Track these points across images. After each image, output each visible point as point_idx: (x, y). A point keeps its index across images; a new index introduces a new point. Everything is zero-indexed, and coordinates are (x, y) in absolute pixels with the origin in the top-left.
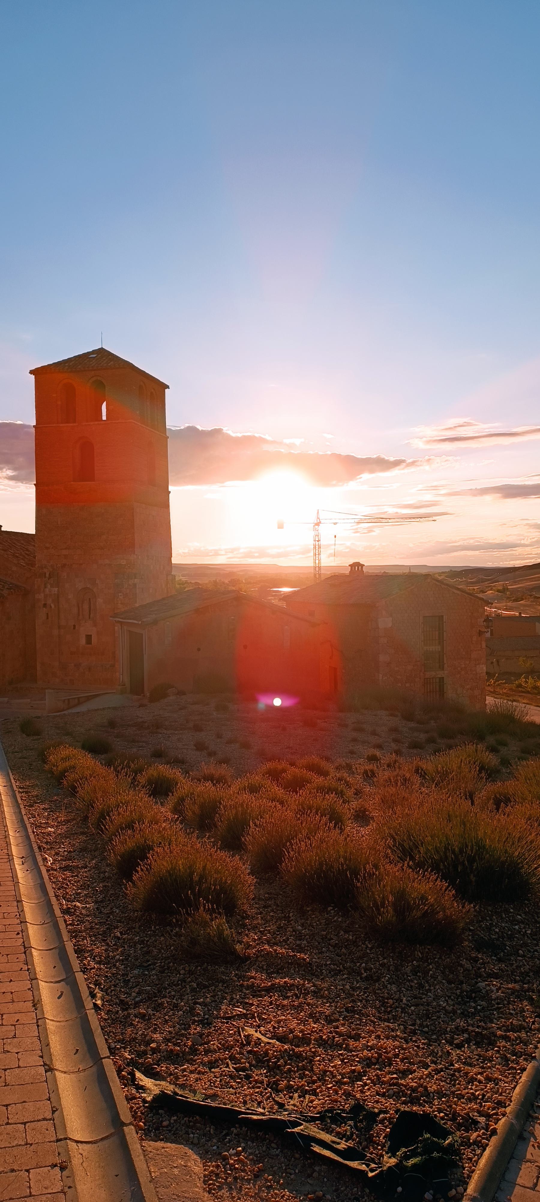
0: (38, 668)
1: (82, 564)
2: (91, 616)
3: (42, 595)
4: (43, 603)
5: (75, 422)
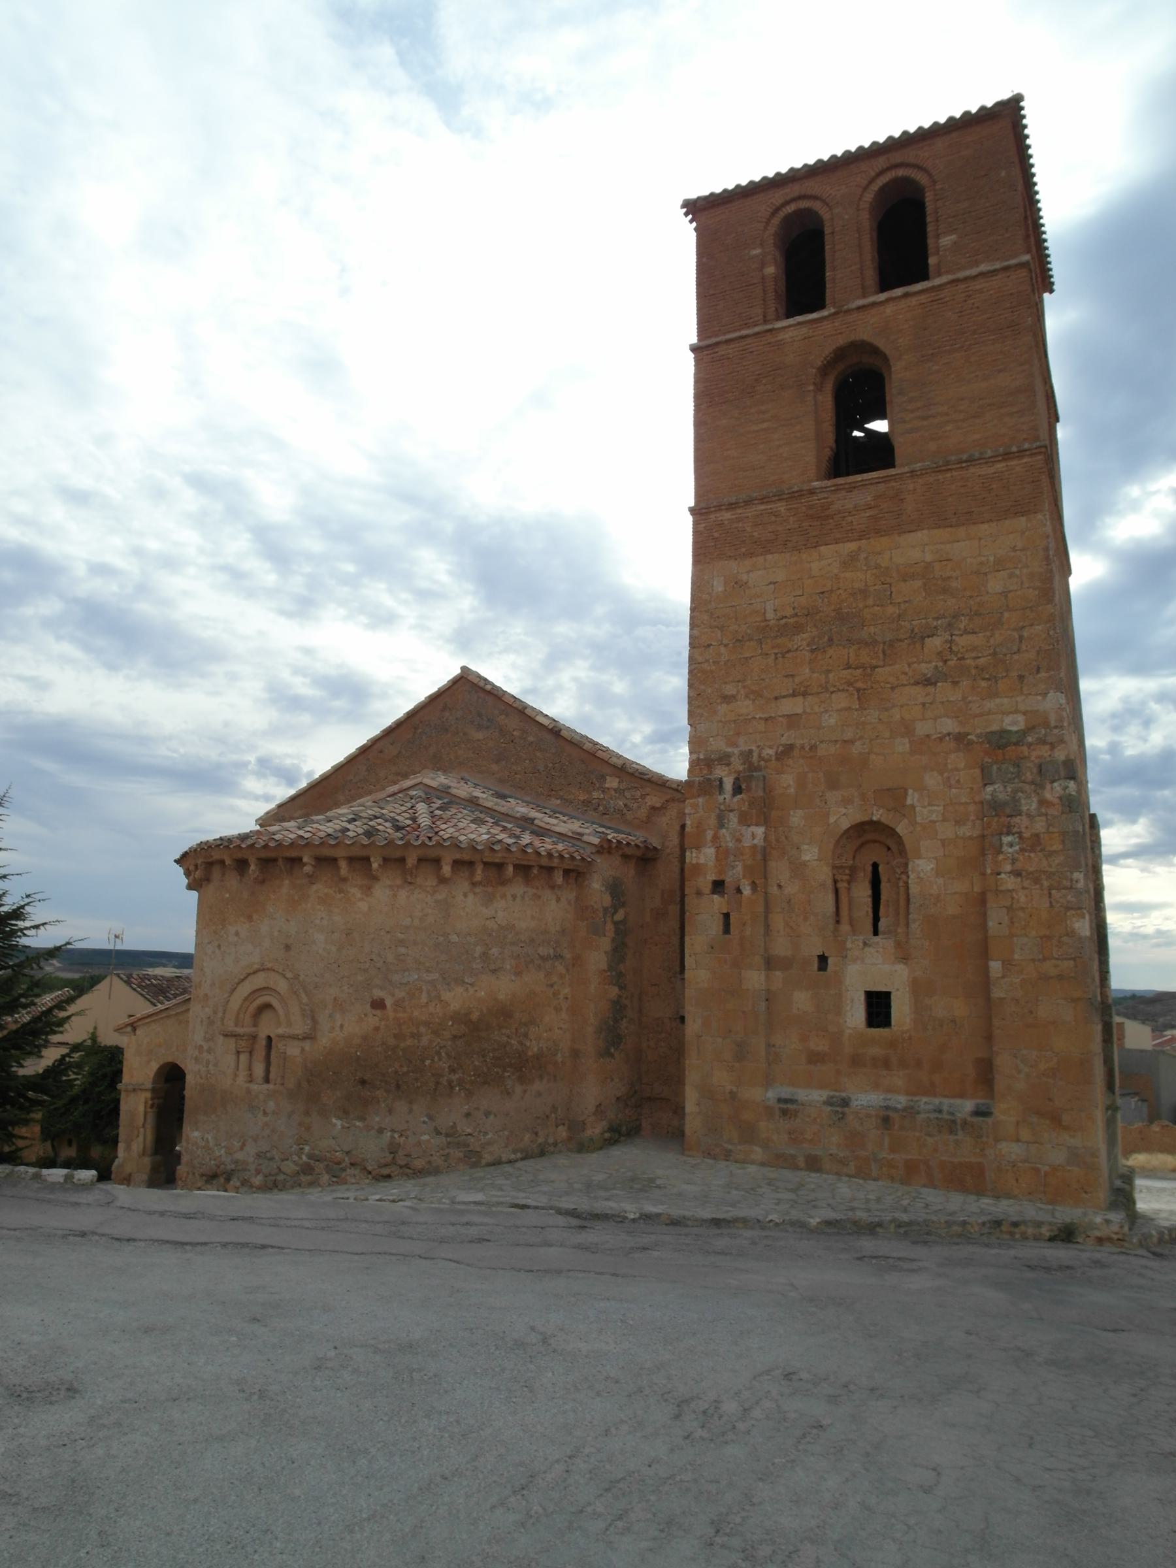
0: (690, 1107)
1: (852, 742)
4: (712, 877)
5: (821, 306)
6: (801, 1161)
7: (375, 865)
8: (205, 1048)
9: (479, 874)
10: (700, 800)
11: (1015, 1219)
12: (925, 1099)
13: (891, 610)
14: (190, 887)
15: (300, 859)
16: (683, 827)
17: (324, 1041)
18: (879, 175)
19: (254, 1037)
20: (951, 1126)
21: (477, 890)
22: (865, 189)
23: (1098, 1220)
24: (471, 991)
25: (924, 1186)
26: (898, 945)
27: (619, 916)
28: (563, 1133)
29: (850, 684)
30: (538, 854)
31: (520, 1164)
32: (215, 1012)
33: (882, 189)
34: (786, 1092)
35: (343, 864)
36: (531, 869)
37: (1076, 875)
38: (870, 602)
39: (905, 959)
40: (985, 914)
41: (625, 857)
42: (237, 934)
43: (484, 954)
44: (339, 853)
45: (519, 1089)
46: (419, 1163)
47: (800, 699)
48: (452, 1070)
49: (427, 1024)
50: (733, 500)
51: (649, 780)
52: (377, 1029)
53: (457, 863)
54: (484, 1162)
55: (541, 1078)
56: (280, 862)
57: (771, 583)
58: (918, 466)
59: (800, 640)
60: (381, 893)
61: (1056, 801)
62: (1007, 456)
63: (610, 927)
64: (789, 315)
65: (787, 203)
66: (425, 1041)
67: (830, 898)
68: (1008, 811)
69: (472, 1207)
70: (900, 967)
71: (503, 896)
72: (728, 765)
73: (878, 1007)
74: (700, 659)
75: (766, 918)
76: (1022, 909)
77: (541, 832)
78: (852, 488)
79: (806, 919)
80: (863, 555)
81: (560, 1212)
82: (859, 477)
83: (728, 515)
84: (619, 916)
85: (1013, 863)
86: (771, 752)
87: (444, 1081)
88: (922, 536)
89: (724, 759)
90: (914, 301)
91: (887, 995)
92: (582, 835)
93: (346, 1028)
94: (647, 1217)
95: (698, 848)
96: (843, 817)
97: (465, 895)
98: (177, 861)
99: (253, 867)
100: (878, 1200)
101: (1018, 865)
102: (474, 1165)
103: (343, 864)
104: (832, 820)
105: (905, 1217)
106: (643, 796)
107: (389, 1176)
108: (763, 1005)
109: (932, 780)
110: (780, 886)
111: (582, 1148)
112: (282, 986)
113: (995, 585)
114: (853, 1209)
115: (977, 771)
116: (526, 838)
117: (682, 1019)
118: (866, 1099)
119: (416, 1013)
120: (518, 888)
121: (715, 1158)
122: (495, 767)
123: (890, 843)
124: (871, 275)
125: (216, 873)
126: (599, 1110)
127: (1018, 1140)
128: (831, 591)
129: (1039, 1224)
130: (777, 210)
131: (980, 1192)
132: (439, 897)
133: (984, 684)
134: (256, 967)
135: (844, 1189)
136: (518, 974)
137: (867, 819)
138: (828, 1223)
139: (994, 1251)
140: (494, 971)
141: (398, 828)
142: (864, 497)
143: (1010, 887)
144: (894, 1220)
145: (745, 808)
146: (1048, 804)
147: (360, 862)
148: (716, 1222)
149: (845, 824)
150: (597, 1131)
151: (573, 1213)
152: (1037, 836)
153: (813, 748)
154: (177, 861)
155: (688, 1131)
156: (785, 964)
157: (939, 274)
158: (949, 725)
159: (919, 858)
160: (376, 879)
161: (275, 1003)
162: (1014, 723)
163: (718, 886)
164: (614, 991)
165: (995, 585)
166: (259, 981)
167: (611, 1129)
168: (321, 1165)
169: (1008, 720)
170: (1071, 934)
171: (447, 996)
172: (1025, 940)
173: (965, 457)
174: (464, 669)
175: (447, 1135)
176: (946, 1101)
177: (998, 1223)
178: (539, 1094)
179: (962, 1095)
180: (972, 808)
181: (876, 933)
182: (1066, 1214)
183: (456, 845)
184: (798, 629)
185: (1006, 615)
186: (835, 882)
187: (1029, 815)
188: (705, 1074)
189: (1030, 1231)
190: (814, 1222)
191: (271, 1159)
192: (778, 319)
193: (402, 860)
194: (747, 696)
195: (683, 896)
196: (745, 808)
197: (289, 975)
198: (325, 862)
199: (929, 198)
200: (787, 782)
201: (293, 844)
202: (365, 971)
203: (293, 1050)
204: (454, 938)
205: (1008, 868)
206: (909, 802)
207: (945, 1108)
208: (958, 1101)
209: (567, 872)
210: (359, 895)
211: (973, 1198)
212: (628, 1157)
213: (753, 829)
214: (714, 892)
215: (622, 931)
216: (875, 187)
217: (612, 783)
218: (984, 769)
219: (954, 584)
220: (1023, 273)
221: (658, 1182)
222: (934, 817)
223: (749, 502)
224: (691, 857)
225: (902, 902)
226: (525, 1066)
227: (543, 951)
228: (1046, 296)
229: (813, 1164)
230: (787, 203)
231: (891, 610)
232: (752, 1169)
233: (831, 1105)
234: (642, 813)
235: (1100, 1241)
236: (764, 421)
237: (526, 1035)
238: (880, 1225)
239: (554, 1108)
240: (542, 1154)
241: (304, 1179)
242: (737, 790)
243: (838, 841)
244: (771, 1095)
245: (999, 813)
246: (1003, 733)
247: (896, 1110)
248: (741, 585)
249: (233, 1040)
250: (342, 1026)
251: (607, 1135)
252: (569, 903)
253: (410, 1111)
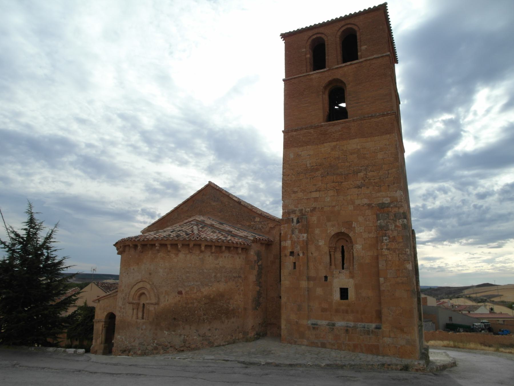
0: (283, 326)
1: (335, 206)
2: (345, 266)
3: (289, 242)
4: (290, 250)
5: (324, 67)
6: (319, 344)
7: (179, 247)
8: (122, 307)
9: (213, 249)
10: (286, 225)
11: (389, 363)
12: (359, 324)
13: (347, 164)
14: (118, 254)
15: (155, 245)
16: (280, 234)
17: (162, 305)
18: (342, 27)
19: (139, 304)
20: (368, 332)
21: (213, 255)
22: (338, 31)
23: (416, 363)
24: (211, 288)
25: (360, 352)
26: (350, 272)
27: (260, 263)
28: (241, 335)
29: (334, 188)
30: (233, 243)
31: (227, 346)
32: (126, 296)
33: (343, 31)
34: (314, 321)
35: (169, 246)
36: (231, 248)
37: (407, 250)
38: (340, 161)
39: (352, 277)
40: (378, 263)
41: (262, 244)
42: (134, 269)
43: (215, 276)
44: (168, 243)
45: (226, 321)
46: (193, 346)
47: (318, 193)
48: (204, 315)
49: (196, 299)
50: (296, 128)
51: (269, 219)
52: (180, 301)
53: (206, 246)
54: (215, 345)
55: (234, 317)
56: (148, 246)
57: (308, 155)
58: (355, 118)
60: (181, 256)
61: (400, 226)
62: (383, 115)
63: (256, 267)
64: (314, 70)
65: (313, 35)
66: (195, 305)
67: (328, 257)
68: (385, 229)
69: (210, 361)
70: (351, 280)
71: (222, 257)
72: (295, 214)
73: (344, 293)
74: (286, 179)
75: (308, 264)
76: (390, 261)
77: (234, 236)
78: (334, 125)
79: (320, 264)
80: (338, 147)
81: (239, 362)
82: (336, 122)
83: (295, 133)
84: (260, 263)
85: (387, 246)
86: (309, 209)
87: (202, 318)
88: (357, 140)
89: (294, 212)
90: (353, 66)
91: (347, 289)
92: (247, 236)
93: (169, 300)
94: (268, 364)
95: (285, 241)
96: (332, 231)
97: (209, 257)
98: (114, 245)
99: (139, 247)
100: (344, 357)
101: (389, 246)
102: (212, 346)
103: (169, 246)
104: (328, 232)
105: (353, 363)
106: (268, 224)
107: (183, 351)
108: (307, 293)
109: (361, 219)
110: (312, 253)
111: (247, 340)
112: (148, 287)
113: (380, 156)
114: (336, 360)
115: (375, 216)
116: (229, 238)
117: (280, 297)
119: (193, 296)
120: (227, 254)
121: (291, 344)
122: (219, 214)
123: (348, 239)
124: (340, 58)
125: (127, 249)
126: (253, 328)
127: (390, 337)
128: (328, 158)
129: (397, 365)
130: (310, 37)
131: (378, 354)
132: (200, 257)
133: (377, 188)
134: (140, 280)
135: (333, 354)
136: (226, 282)
137: (340, 231)
138: (328, 365)
139: (382, 374)
140: (218, 282)
141: (187, 234)
142: (338, 128)
143: (386, 253)
144: (349, 364)
145: (300, 228)
146: (398, 227)
147: (174, 245)
148: (291, 365)
149: (333, 233)
150: (253, 335)
151: (243, 363)
152: (394, 237)
153: (322, 208)
154: (114, 245)
155: (282, 335)
157: (361, 58)
158: (366, 201)
159: (357, 244)
160: (180, 251)
161: (146, 292)
162: (387, 200)
163: (292, 253)
164: (258, 288)
165: (380, 156)
166: (140, 285)
167: (257, 334)
168: (161, 347)
169: (384, 199)
170: (406, 269)
171: (203, 290)
172: (391, 271)
173: (370, 115)
174: (210, 182)
175: (202, 337)
176: (367, 324)
177: (383, 365)
178: (233, 323)
179: (371, 322)
180: (373, 228)
181: (343, 268)
182: (406, 361)
183: (206, 240)
184: (317, 170)
185: (384, 166)
186: (330, 252)
187: (391, 230)
188: (288, 316)
189: (394, 367)
190: (323, 365)
191: (144, 345)
192: (311, 71)
193: (188, 245)
194: (301, 192)
195: (280, 257)
196: (300, 228)
197: (151, 283)
198: (163, 245)
199: (358, 34)
200: (314, 219)
201: (152, 240)
202: (176, 282)
203: (152, 308)
204: (205, 271)
205: (385, 247)
206: (353, 226)
207: (366, 326)
208: (370, 324)
209: (242, 249)
210: (174, 257)
211: (376, 356)
212: (262, 343)
213: (303, 234)
214: (290, 255)
215: (261, 268)
216: (341, 30)
217: (257, 219)
218: (377, 215)
219: (367, 156)
220: (388, 58)
221: (272, 352)
222: (361, 231)
223: (302, 129)
224: (283, 244)
225: (351, 259)
226: (229, 313)
227: (234, 275)
228: (396, 64)
229: (323, 345)
230: (313, 35)
231: (347, 164)
232: (303, 347)
233: (329, 325)
235: (417, 370)
236: (306, 103)
237: (229, 303)
238: (345, 365)
239: (238, 327)
240: (234, 342)
241: (155, 352)
242: (298, 222)
243: (330, 239)
244: (309, 322)
245: (382, 230)
246: (383, 204)
247: (350, 327)
248: (299, 156)
249: (131, 305)
250: (168, 300)
251: (256, 336)
252: (243, 259)
253: (190, 329)
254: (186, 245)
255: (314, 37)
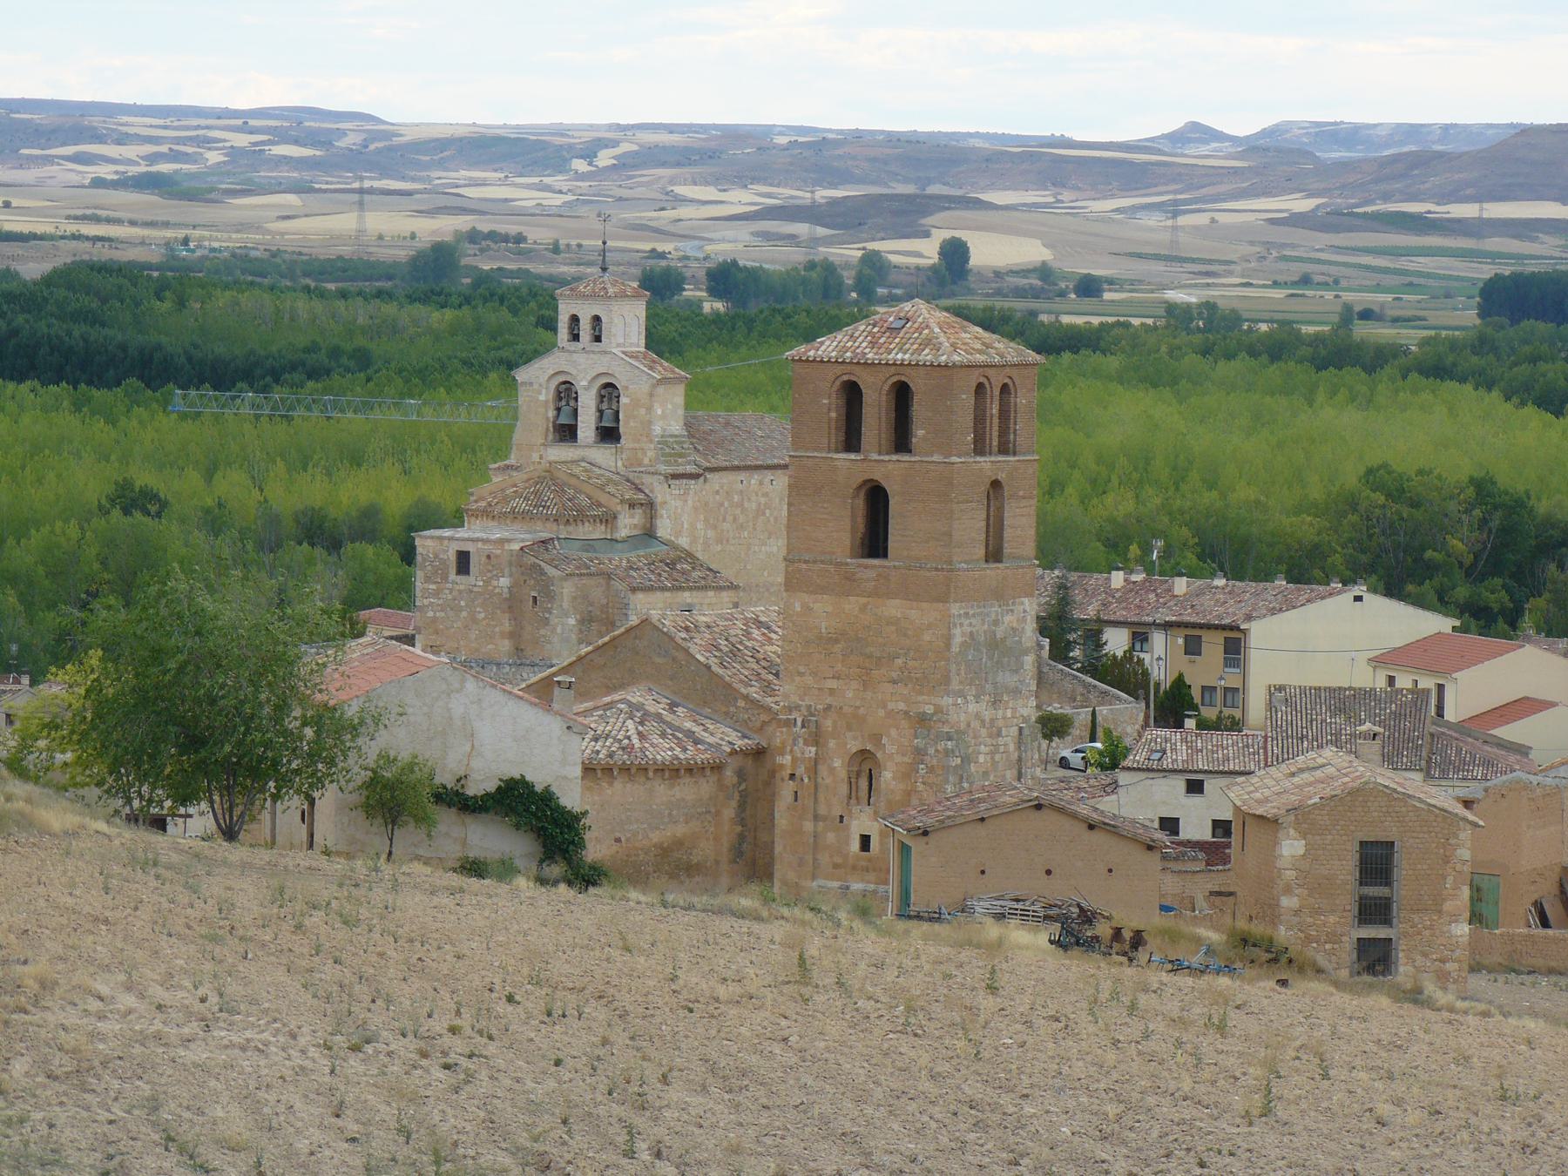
3: (789, 758)
27: (743, 787)
53: (656, 771)
59: (837, 648)
60: (618, 785)
62: (937, 569)
73: (865, 841)
77: (697, 742)
89: (798, 708)
96: (854, 746)
109: (893, 732)
113: (927, 637)
118: (857, 886)
142: (872, 574)
156: (824, 819)
158: (902, 706)
162: (929, 709)
164: (739, 829)
165: (927, 637)
171: (651, 835)
184: (837, 641)
192: (837, 451)
200: (828, 724)
215: (744, 796)
217: (741, 703)
223: (815, 562)
234: (758, 724)
245: (919, 753)
254: (625, 770)
255: (845, 378)
